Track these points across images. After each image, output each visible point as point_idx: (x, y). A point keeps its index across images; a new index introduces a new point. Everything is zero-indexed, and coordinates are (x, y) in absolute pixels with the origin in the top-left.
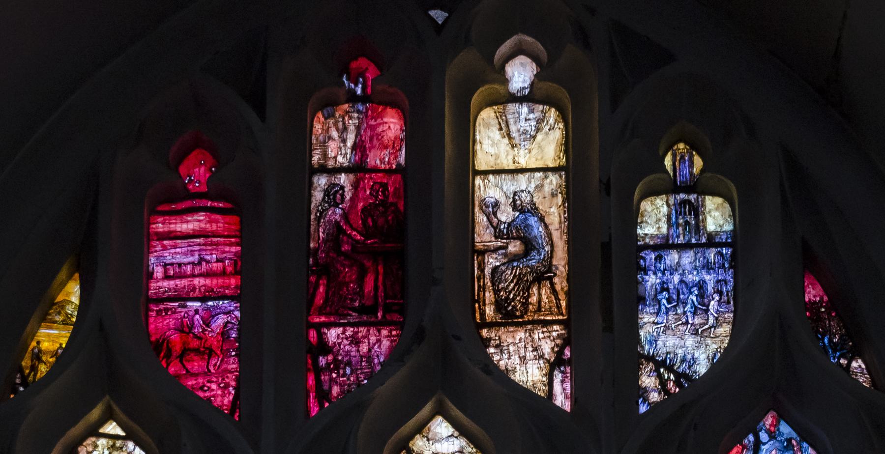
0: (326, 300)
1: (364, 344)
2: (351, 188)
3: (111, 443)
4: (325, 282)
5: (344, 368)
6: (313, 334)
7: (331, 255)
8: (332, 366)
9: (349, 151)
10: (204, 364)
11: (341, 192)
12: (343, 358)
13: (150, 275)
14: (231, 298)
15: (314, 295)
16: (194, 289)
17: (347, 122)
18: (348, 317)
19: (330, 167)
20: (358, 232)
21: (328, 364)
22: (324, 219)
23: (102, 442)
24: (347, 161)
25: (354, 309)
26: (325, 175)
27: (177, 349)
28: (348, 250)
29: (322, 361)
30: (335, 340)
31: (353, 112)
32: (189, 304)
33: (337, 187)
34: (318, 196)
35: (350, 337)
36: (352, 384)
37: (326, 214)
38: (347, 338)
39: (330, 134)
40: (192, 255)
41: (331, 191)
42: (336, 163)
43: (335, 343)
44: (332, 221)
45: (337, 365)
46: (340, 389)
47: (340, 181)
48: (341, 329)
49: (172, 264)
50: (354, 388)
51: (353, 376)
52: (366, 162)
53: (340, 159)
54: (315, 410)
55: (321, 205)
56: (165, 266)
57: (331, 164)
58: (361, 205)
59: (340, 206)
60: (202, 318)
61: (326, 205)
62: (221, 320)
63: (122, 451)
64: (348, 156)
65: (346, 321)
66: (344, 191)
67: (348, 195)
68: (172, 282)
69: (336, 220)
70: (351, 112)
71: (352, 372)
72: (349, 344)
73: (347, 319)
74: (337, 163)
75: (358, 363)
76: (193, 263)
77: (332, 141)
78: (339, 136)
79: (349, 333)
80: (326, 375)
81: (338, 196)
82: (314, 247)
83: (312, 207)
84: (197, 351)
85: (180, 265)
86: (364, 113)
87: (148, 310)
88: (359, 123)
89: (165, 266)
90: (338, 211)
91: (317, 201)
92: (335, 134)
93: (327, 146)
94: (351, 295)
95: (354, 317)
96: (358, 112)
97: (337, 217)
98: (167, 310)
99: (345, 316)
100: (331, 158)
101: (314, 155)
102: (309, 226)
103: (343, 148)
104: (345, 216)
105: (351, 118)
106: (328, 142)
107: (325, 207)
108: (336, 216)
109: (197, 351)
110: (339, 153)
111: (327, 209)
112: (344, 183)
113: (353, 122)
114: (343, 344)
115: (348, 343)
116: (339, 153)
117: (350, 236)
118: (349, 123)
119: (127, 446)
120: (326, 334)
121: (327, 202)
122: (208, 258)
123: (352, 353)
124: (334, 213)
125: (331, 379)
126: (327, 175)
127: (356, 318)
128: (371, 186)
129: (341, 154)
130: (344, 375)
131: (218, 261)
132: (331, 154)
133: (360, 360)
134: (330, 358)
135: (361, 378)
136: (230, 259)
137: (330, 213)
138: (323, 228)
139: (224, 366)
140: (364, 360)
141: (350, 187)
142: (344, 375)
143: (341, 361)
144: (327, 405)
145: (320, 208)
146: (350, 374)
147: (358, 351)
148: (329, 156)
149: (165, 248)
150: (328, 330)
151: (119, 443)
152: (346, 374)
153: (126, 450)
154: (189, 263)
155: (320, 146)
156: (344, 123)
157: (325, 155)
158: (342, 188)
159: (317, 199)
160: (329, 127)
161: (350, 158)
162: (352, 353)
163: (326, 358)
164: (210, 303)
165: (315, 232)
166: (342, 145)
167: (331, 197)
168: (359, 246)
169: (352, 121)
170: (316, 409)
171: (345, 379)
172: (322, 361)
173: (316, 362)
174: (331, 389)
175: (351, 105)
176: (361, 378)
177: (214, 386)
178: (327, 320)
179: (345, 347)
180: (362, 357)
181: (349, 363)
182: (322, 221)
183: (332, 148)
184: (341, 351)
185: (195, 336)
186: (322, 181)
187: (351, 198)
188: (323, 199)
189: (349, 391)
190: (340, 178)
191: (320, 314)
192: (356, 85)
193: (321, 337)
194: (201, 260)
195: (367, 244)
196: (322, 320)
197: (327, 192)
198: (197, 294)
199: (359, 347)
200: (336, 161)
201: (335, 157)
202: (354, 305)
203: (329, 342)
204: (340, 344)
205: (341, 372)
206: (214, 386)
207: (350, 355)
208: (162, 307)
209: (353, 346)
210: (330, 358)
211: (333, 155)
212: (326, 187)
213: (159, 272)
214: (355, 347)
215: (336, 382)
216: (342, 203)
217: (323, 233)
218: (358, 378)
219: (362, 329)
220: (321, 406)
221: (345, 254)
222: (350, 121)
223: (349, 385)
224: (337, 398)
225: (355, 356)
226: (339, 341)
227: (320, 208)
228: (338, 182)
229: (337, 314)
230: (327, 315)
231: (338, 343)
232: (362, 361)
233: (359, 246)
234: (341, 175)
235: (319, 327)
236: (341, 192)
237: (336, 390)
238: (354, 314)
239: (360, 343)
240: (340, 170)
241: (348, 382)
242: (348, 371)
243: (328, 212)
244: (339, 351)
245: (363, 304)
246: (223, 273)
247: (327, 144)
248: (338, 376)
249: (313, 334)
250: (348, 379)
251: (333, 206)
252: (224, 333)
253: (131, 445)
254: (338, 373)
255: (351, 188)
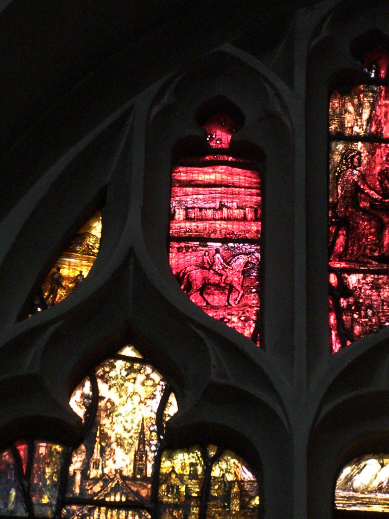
0: (346, 248)
1: (385, 290)
2: (367, 154)
3: (128, 365)
4: (344, 232)
5: (366, 310)
6: (333, 279)
7: (350, 210)
8: (353, 308)
9: (365, 123)
10: (224, 298)
11: (357, 157)
12: (364, 301)
13: (172, 216)
14: (251, 241)
15: (334, 244)
16: (215, 231)
17: (362, 100)
18: (368, 265)
19: (347, 135)
20: (376, 192)
21: (349, 306)
22: (342, 178)
23: (120, 364)
24: (363, 131)
25: (375, 259)
26: (342, 141)
27: (198, 283)
28: (367, 206)
29: (343, 303)
30: (356, 285)
31: (368, 91)
32: (209, 244)
33: (355, 152)
34: (337, 158)
35: (371, 283)
36: (374, 325)
37: (344, 174)
38: (367, 284)
39: (346, 108)
40: (214, 202)
41: (348, 156)
42: (352, 132)
43: (355, 287)
44: (350, 181)
45: (358, 307)
46: (362, 329)
47: (357, 147)
48: (361, 275)
49: (193, 208)
50: (375, 329)
51: (375, 318)
52: (381, 133)
53: (356, 129)
54: (336, 347)
55: (339, 166)
56: (187, 209)
57: (348, 132)
58: (378, 168)
59: (358, 169)
60: (223, 257)
61: (344, 167)
62: (242, 260)
63: (140, 373)
64: (365, 127)
65: (367, 268)
66: (361, 157)
67: (365, 159)
68: (194, 224)
69: (354, 180)
70: (366, 92)
71: (373, 314)
72: (370, 289)
73: (367, 267)
74: (354, 132)
75: (379, 307)
76: (214, 209)
77: (348, 114)
78: (354, 110)
79: (369, 279)
80: (348, 316)
81: (356, 160)
82: (333, 202)
83: (330, 168)
84: (217, 286)
85: (201, 209)
86: (379, 93)
87: (168, 247)
88: (373, 101)
89: (187, 209)
90: (355, 172)
91: (335, 163)
92: (351, 108)
93: (344, 117)
94: (370, 245)
95: (375, 265)
96: (373, 91)
97: (355, 178)
98: (187, 248)
99: (365, 264)
100: (348, 127)
101: (331, 124)
102: (328, 183)
103: (359, 120)
104: (363, 177)
105: (365, 96)
106: (344, 115)
107: (343, 168)
108: (354, 176)
109: (217, 286)
110: (356, 124)
111: (345, 170)
112: (361, 149)
113: (368, 99)
114: (364, 289)
115: (369, 288)
116: (356, 124)
117: (367, 194)
118: (364, 100)
119: (145, 369)
120: (346, 279)
121: (345, 165)
122: (229, 205)
123: (373, 297)
124: (352, 174)
125: (353, 319)
126: (344, 142)
127: (377, 266)
128: (387, 154)
129: (357, 125)
130: (366, 316)
131: (238, 208)
132: (348, 125)
133: (381, 304)
134: (351, 300)
135: (382, 320)
136: (251, 207)
137: (347, 174)
138: (341, 186)
139: (244, 302)
140: (385, 304)
141: (366, 153)
142: (366, 316)
143: (362, 304)
144: (349, 343)
145: (338, 169)
146: (372, 316)
147: (379, 296)
148: (346, 126)
149: (187, 195)
150: (349, 275)
151: (137, 366)
152: (368, 316)
153: (144, 372)
154: (210, 208)
155: (337, 117)
156: (359, 100)
157: (342, 125)
158: (359, 153)
159: (335, 161)
160: (345, 102)
161: (366, 129)
162: (373, 297)
163: (347, 300)
164: (231, 245)
165: (333, 188)
166: (358, 117)
167: (349, 161)
168: (377, 203)
169: (367, 98)
170: (338, 346)
171: (367, 320)
172: (343, 303)
173: (337, 303)
174: (352, 328)
175: (365, 86)
176: (382, 320)
177: (235, 319)
178: (348, 266)
179: (365, 291)
180: (383, 301)
181: (370, 307)
182: (340, 180)
183: (349, 118)
184: (362, 295)
185: (216, 273)
186: (340, 147)
187: (367, 162)
188: (341, 161)
189: (371, 332)
190: (357, 145)
191: (340, 261)
192: (370, 70)
193: (342, 281)
194: (222, 206)
195: (385, 202)
196: (342, 266)
197: (344, 156)
198: (218, 235)
199: (380, 292)
200: (352, 131)
201: (352, 128)
202: (374, 254)
203: (350, 286)
204: (360, 288)
205: (363, 312)
206: (235, 319)
207: (371, 299)
208: (183, 245)
209: (374, 291)
210: (351, 300)
211: (349, 125)
212: (343, 151)
213: (180, 214)
214: (376, 292)
215: (358, 323)
216: (359, 166)
217: (342, 190)
218: (380, 320)
219: (382, 276)
220: (343, 344)
221: (364, 210)
222: (365, 99)
223: (371, 326)
224: (359, 336)
225: (376, 301)
226: (360, 286)
227: (338, 169)
228: (355, 149)
229: (357, 261)
230: (347, 261)
231: (359, 287)
232: (383, 305)
233: (377, 203)
234: (358, 142)
235: (339, 273)
236: (357, 157)
237: (357, 329)
238: (374, 262)
239: (381, 289)
240: (357, 138)
241: (370, 323)
242: (370, 312)
243: (346, 173)
244: (360, 294)
245: (383, 255)
246: (244, 219)
247: (343, 116)
248: (360, 317)
249: (333, 279)
250: (370, 320)
251: (351, 167)
252: (245, 273)
253: (149, 370)
254: (360, 315)
255: (367, 154)
